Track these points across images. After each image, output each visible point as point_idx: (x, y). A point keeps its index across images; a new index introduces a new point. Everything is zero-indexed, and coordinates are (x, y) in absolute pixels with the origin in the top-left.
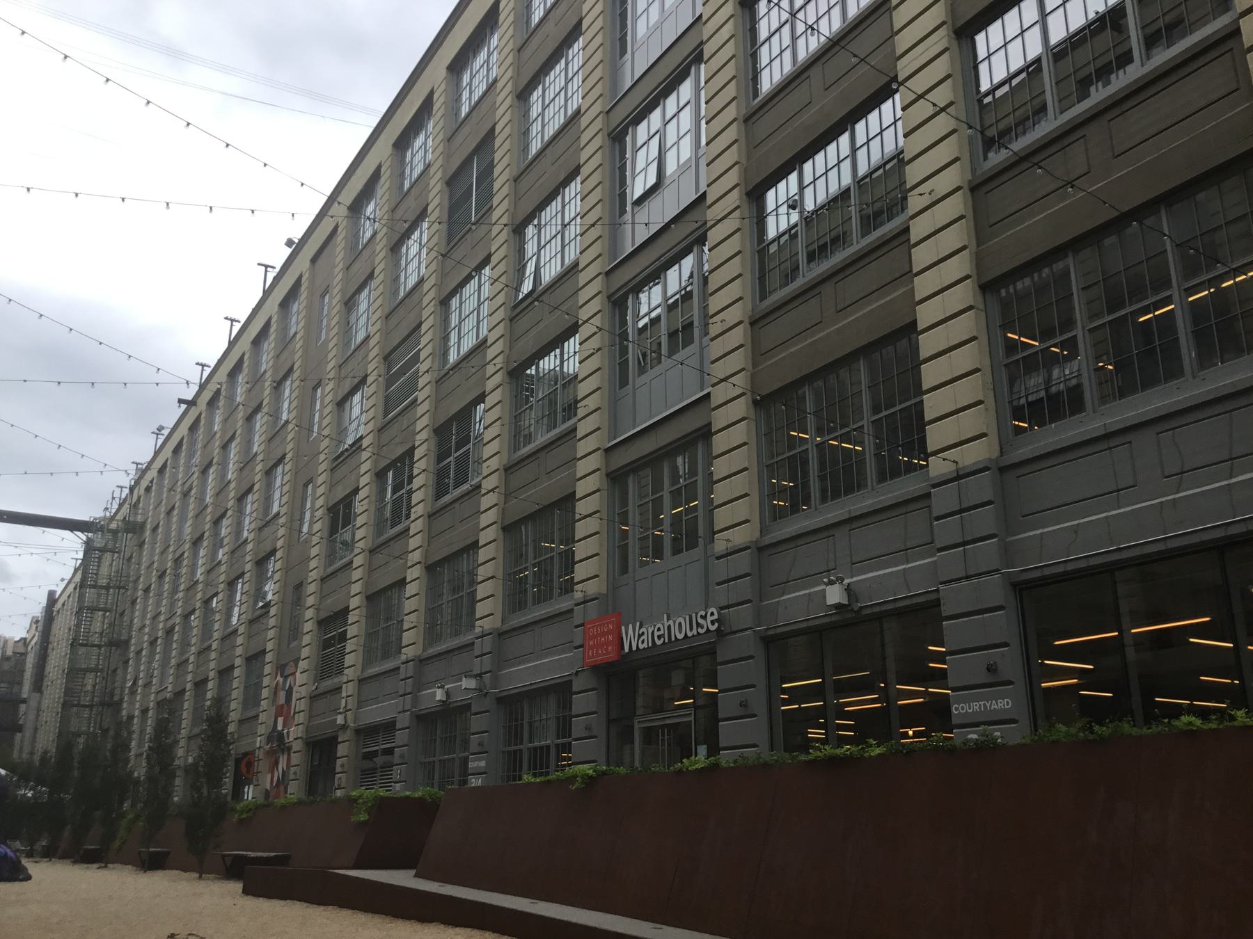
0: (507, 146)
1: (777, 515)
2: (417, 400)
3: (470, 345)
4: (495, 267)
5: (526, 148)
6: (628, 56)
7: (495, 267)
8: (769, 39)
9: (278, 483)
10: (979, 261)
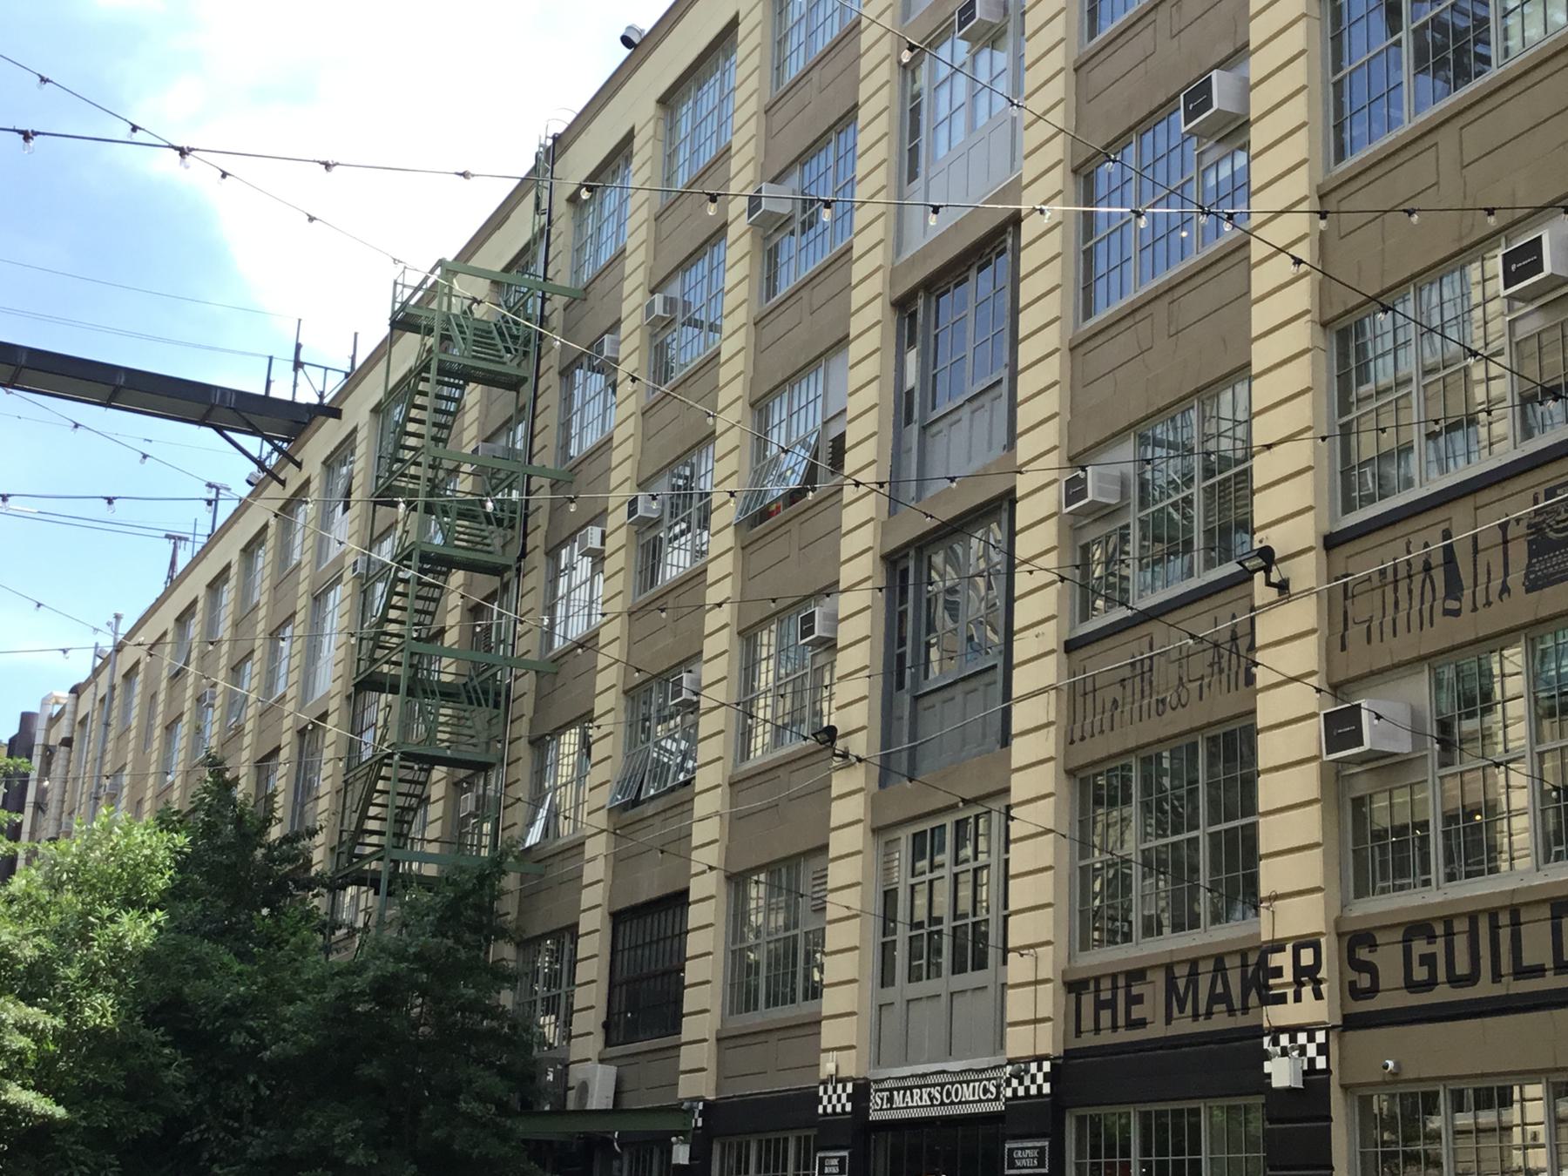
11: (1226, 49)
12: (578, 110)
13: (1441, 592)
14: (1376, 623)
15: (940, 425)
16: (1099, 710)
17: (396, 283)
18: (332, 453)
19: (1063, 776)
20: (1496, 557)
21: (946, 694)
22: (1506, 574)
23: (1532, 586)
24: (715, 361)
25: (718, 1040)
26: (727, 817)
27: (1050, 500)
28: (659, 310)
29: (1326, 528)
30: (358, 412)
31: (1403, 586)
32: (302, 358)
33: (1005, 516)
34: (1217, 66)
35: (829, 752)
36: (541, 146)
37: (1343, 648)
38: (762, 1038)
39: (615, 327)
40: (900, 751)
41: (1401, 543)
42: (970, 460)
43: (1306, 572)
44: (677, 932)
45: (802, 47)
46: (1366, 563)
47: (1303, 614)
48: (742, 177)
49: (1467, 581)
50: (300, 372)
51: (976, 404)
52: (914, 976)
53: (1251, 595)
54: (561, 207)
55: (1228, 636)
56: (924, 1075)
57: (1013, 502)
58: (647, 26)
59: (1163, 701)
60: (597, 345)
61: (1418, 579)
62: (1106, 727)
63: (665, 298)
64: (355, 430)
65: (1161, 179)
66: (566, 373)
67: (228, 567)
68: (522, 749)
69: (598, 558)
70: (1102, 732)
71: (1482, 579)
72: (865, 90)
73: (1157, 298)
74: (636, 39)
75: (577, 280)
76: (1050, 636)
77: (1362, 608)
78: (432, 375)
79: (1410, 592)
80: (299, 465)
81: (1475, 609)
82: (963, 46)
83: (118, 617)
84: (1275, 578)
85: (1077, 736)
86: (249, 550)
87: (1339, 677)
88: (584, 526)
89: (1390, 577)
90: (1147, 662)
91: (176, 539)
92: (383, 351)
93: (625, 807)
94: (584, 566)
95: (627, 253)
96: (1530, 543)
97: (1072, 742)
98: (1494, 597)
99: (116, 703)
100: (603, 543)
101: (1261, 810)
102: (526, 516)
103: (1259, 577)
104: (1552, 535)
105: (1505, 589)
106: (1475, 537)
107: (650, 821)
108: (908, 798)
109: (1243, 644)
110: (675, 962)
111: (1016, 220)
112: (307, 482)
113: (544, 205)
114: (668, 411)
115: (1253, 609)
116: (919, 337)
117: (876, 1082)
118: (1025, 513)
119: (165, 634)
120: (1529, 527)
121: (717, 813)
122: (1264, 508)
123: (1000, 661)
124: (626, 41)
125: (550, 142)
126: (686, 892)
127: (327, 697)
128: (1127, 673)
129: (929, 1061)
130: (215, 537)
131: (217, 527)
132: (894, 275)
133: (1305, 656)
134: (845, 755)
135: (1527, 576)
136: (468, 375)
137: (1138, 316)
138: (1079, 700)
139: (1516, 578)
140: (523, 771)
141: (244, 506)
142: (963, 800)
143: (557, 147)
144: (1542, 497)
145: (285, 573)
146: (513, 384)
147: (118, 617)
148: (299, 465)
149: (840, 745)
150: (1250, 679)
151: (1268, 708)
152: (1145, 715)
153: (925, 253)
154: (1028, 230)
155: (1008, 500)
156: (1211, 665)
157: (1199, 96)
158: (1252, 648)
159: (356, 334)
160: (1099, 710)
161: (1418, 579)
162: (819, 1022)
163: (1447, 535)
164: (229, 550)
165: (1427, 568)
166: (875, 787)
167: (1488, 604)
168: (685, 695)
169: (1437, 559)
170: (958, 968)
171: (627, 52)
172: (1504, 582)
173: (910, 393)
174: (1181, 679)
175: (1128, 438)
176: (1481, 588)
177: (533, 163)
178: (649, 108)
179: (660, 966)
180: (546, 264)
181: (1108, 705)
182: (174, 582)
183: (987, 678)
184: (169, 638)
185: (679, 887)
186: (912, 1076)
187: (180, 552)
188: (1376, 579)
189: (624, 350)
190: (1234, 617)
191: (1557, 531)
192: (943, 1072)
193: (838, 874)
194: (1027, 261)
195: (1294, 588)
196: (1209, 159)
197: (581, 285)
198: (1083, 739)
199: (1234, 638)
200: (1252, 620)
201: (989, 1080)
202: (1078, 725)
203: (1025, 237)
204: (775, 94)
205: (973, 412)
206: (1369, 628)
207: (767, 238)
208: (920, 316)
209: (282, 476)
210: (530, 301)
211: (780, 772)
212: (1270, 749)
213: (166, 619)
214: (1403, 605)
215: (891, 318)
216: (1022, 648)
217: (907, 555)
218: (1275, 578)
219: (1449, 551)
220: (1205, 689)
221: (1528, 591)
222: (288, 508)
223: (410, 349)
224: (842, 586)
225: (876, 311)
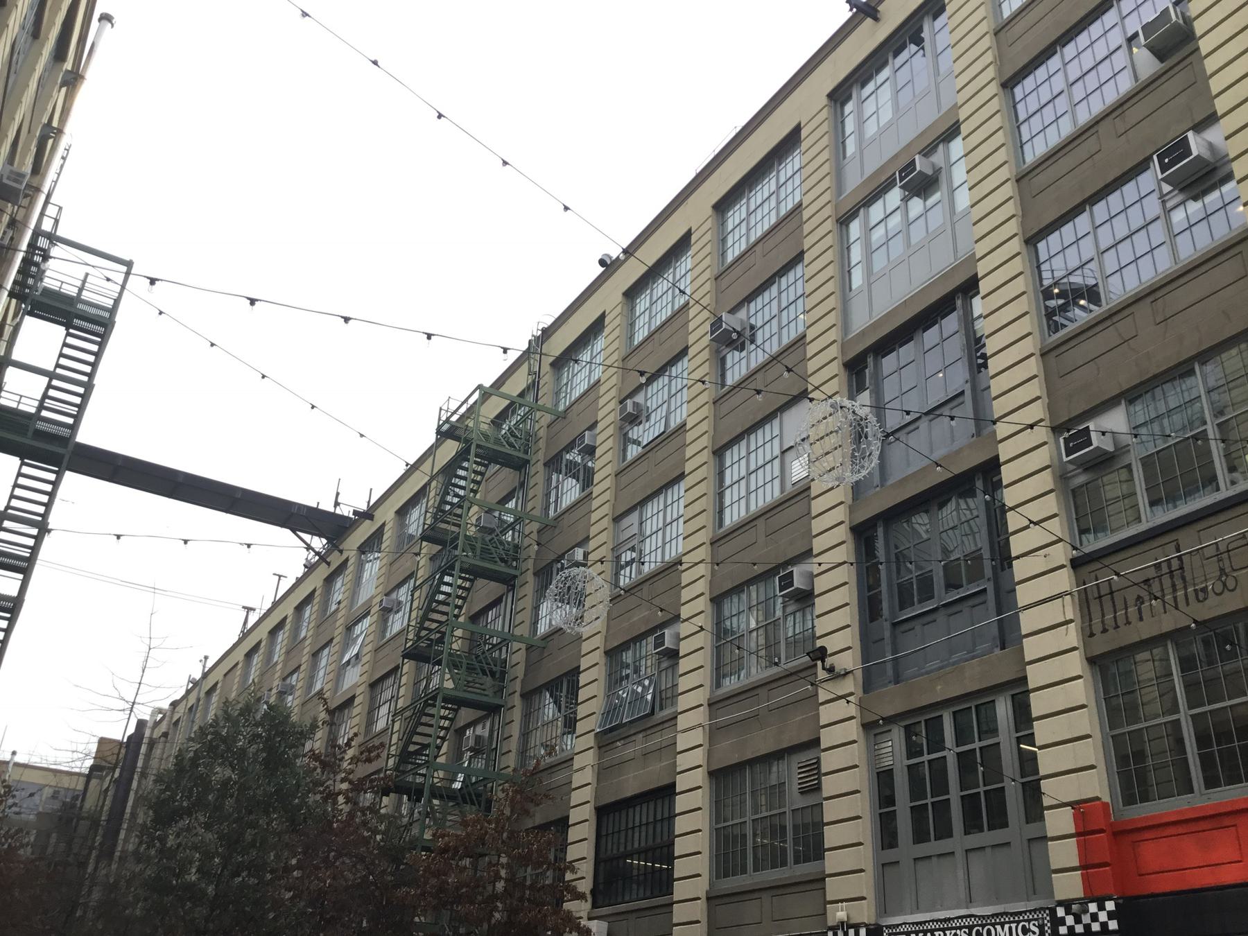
2: (592, 493)
3: (573, 499)
4: (691, 359)
7: (691, 359)
9: (323, 662)
12: (557, 316)
17: (441, 409)
18: (365, 541)
19: (1085, 662)
24: (683, 429)
25: (708, 899)
26: (707, 728)
28: (630, 409)
30: (387, 515)
32: (339, 501)
36: (533, 336)
38: (756, 895)
40: (884, 662)
42: (953, 441)
44: (666, 815)
45: (774, 211)
50: (338, 507)
52: (920, 836)
54: (546, 367)
56: (949, 920)
59: (1204, 590)
60: (581, 436)
63: (634, 402)
64: (384, 525)
67: (285, 618)
68: (517, 700)
74: (609, 262)
83: (206, 658)
85: (1097, 628)
86: (299, 608)
88: (573, 547)
90: (1164, 566)
91: (249, 610)
92: (430, 452)
93: (604, 732)
95: (601, 382)
97: (1092, 635)
99: (199, 708)
107: (633, 738)
108: (892, 701)
110: (665, 838)
112: (347, 560)
117: (887, 927)
119: (237, 664)
121: (700, 725)
124: (602, 262)
125: (540, 333)
126: (673, 785)
127: (356, 686)
128: (1152, 573)
129: (958, 907)
130: (276, 604)
131: (277, 599)
140: (517, 714)
141: (299, 581)
142: (883, 719)
143: (547, 333)
145: (325, 618)
147: (206, 658)
148: (341, 552)
153: (863, 333)
159: (371, 490)
162: (824, 879)
164: (288, 609)
166: (860, 692)
168: (668, 643)
171: (602, 269)
175: (1119, 403)
177: (527, 346)
178: (618, 297)
179: (650, 842)
182: (245, 635)
184: (240, 666)
185: (666, 781)
186: (933, 921)
187: (250, 617)
189: (599, 440)
192: (970, 916)
198: (1117, 627)
201: (1029, 921)
204: (721, 268)
207: (718, 351)
209: (328, 560)
211: (759, 691)
213: (239, 655)
215: (844, 375)
217: (874, 527)
222: (330, 580)
223: (451, 448)
224: (815, 552)
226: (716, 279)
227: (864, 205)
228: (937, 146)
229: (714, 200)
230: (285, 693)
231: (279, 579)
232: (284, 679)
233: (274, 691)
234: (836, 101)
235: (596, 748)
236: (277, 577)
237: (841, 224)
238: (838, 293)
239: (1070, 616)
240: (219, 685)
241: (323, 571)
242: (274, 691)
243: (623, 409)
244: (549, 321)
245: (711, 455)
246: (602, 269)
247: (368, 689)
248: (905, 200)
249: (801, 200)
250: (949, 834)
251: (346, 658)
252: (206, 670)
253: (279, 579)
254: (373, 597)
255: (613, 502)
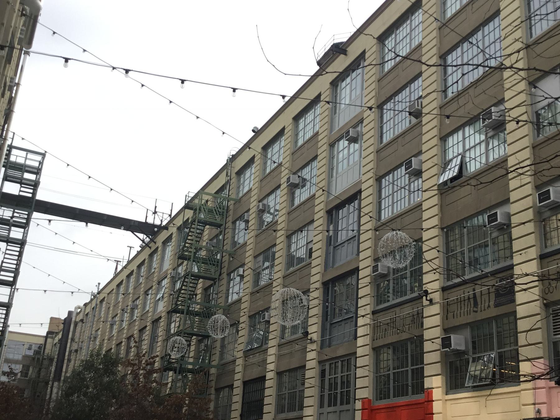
0: (290, 133)
1: (377, 305)
5: (296, 142)
6: (337, 115)
8: (386, 122)
10: (441, 220)
11: (416, 151)
12: (240, 148)
13: (472, 306)
14: (455, 313)
15: (340, 247)
16: (381, 331)
18: (165, 240)
20: (486, 297)
21: (340, 324)
22: (489, 302)
23: (496, 306)
27: (368, 271)
28: (261, 207)
29: (442, 285)
30: (173, 230)
31: (463, 303)
32: (157, 210)
33: (356, 274)
34: (413, 156)
35: (306, 339)
37: (447, 319)
39: (248, 210)
41: (462, 291)
43: (436, 297)
46: (454, 296)
47: (436, 309)
48: (285, 173)
49: (479, 303)
51: (349, 242)
53: (422, 302)
54: (234, 175)
55: (416, 313)
57: (359, 271)
58: (259, 127)
61: (466, 301)
62: (383, 336)
64: (172, 234)
65: (399, 185)
66: (234, 223)
67: (133, 271)
69: (242, 277)
70: (382, 338)
71: (483, 303)
72: (319, 151)
73: (398, 217)
74: (256, 131)
75: (238, 197)
76: (368, 309)
77: (453, 308)
78: (196, 223)
79: (464, 304)
80: (155, 243)
81: (481, 311)
82: (346, 143)
83: (99, 284)
84: (428, 298)
87: (446, 327)
89: (459, 300)
94: (238, 279)
96: (495, 294)
97: (374, 340)
98: (486, 308)
99: (97, 309)
100: (243, 273)
101: (425, 363)
102: (222, 264)
103: (424, 298)
104: (501, 292)
105: (489, 306)
106: (481, 291)
107: (255, 355)
108: (330, 353)
109: (420, 315)
111: (360, 192)
112: (158, 248)
113: (229, 174)
114: (263, 236)
115: (423, 306)
116: (334, 221)
118: (362, 274)
119: (113, 290)
120: (495, 289)
122: (426, 278)
123: (354, 315)
124: (253, 131)
125: (231, 157)
127: (161, 312)
128: (389, 321)
130: (129, 262)
131: (130, 259)
132: (327, 203)
133: (437, 320)
134: (311, 339)
135: (494, 303)
136: (205, 223)
137: (393, 222)
138: (376, 328)
139: (492, 303)
141: (139, 253)
143: (233, 158)
144: (498, 281)
146: (219, 226)
147: (99, 284)
148: (155, 243)
149: (309, 337)
150: (422, 326)
151: (427, 335)
152: (394, 334)
154: (364, 195)
155: (357, 270)
156: (412, 321)
157: (409, 164)
158: (423, 317)
160: (381, 331)
161: (466, 301)
163: (474, 290)
164: (133, 266)
165: (469, 299)
166: (319, 350)
167: (485, 310)
168: (266, 319)
169: (472, 296)
170: (342, 404)
171: (253, 134)
172: (489, 304)
173: (331, 236)
174: (404, 324)
176: (483, 305)
177: (226, 162)
180: (229, 191)
181: (384, 331)
182: (116, 275)
183: (351, 320)
184: (114, 291)
188: (455, 300)
190: (418, 308)
191: (503, 291)
193: (308, 374)
194: (363, 203)
195: (434, 302)
196: (412, 180)
197: (238, 198)
198: (377, 339)
199: (418, 314)
200: (423, 309)
202: (376, 335)
203: (363, 197)
205: (348, 244)
206: (454, 314)
207: (291, 189)
208: (334, 216)
210: (224, 202)
212: (427, 346)
213: (114, 285)
214: (463, 308)
215: (326, 216)
216: (361, 312)
218: (428, 298)
219: (474, 294)
220: (410, 327)
221: (495, 307)
222: (151, 255)
225: (322, 213)
226: (292, 154)
227: (337, 141)
228: (359, 124)
229: (293, 116)
230: (134, 309)
231: (130, 249)
232: (134, 302)
233: (129, 307)
234: (334, 86)
235: (244, 357)
236: (129, 248)
237: (331, 146)
238: (327, 179)
239: (368, 333)
240: (106, 299)
241: (148, 251)
242: (129, 307)
243: (259, 206)
244: (234, 153)
245: (286, 238)
246: (253, 134)
247: (166, 314)
248: (349, 144)
249: (318, 130)
250: (335, 405)
251: (158, 298)
252: (99, 290)
253: (130, 249)
254: (167, 270)
255: (254, 249)
